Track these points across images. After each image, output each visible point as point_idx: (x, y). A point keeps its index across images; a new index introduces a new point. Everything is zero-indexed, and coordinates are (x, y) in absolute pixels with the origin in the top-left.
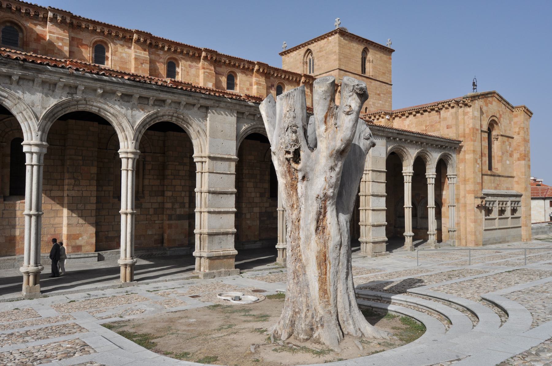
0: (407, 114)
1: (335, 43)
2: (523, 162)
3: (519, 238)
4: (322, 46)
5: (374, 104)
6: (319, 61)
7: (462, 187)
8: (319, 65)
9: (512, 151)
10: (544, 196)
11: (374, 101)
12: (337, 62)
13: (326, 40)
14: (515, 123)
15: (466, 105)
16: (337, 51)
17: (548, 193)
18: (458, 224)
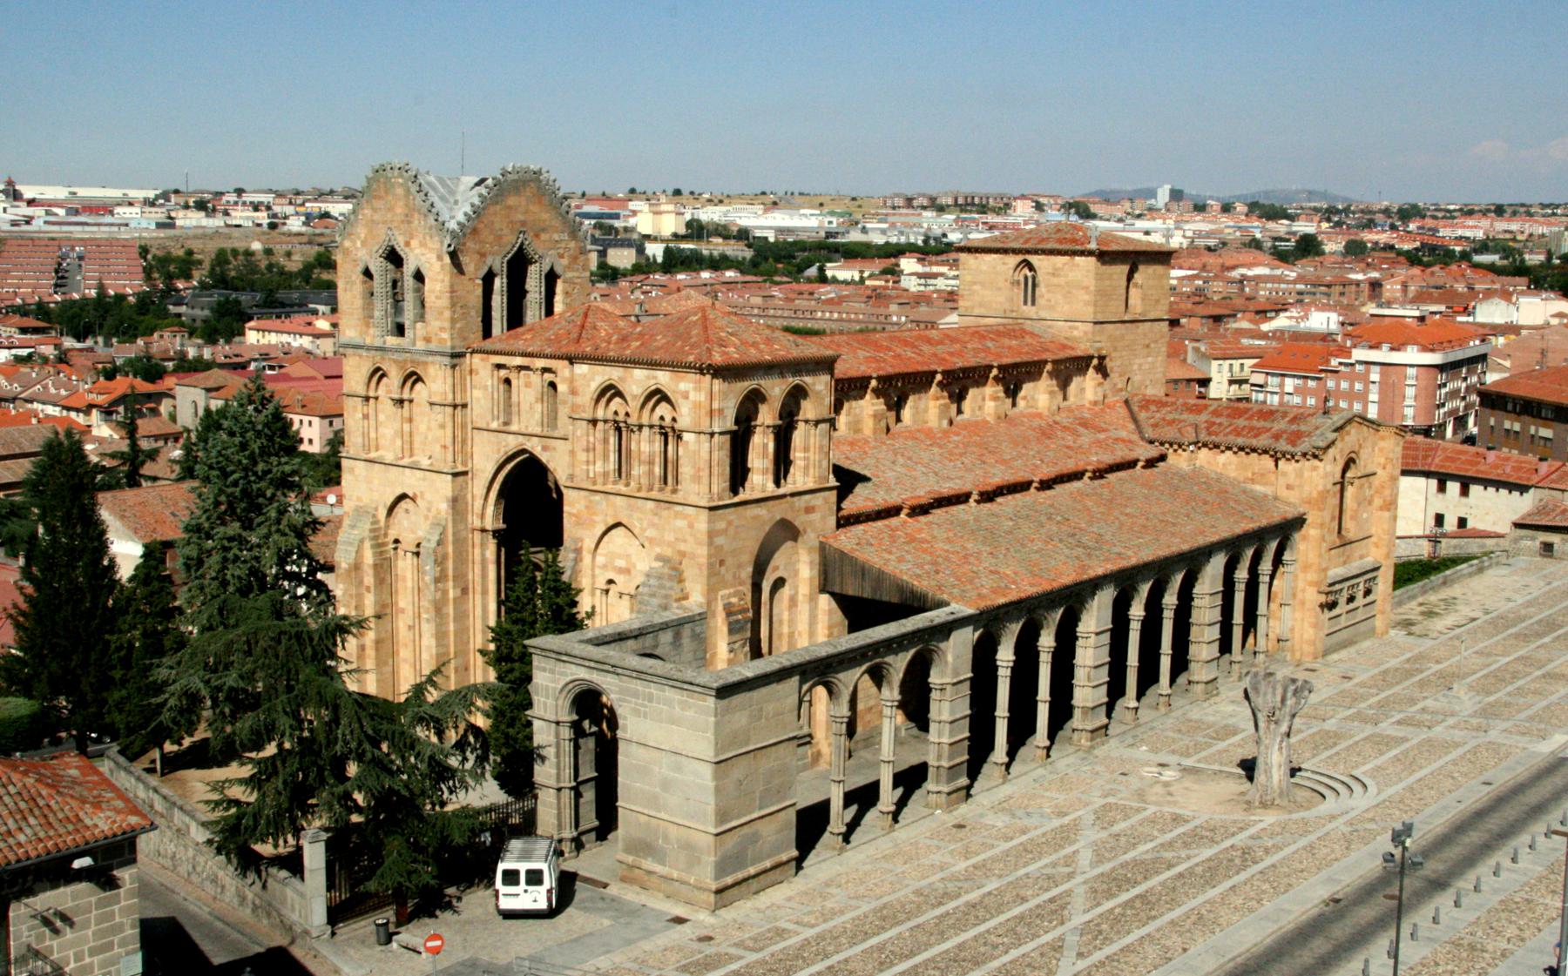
0: (1223, 448)
1: (1088, 271)
2: (1386, 514)
3: (1372, 632)
4: (1059, 265)
5: (1140, 365)
6: (1049, 291)
7: (1301, 576)
8: (1049, 301)
9: (1372, 496)
10: (1426, 468)
11: (1141, 361)
12: (1091, 309)
13: (1066, 258)
14: (1381, 450)
15: (1315, 456)
16: (1092, 288)
17: (1437, 461)
18: (1292, 629)
